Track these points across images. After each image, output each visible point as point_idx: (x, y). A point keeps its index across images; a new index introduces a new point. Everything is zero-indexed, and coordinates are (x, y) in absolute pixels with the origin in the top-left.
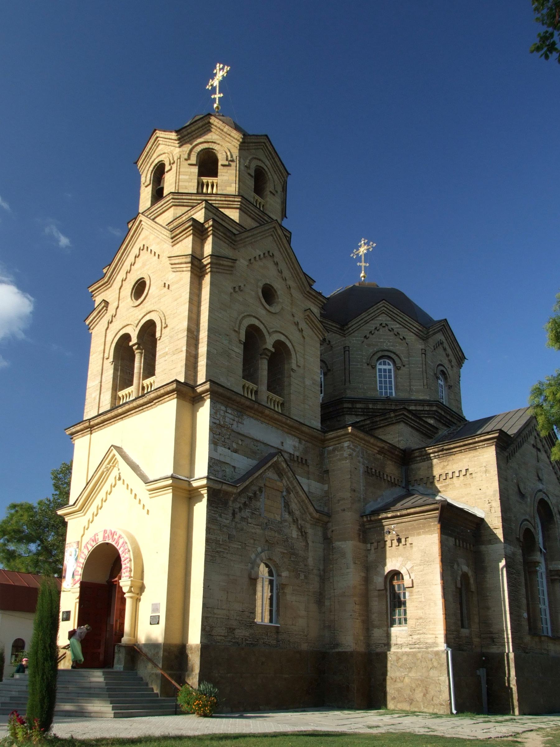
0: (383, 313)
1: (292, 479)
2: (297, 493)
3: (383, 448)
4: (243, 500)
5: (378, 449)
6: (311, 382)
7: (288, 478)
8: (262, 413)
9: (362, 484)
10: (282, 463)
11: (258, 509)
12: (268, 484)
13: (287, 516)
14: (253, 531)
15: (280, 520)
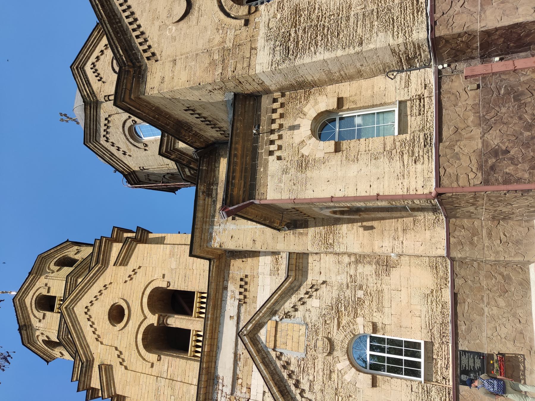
0: (96, 140)
1: (261, 315)
2: (274, 304)
3: (203, 192)
4: (293, 388)
5: (207, 199)
6: (173, 259)
7: (261, 318)
8: (208, 368)
9: (246, 227)
10: (248, 328)
11: (298, 361)
12: (272, 345)
13: (299, 314)
14: (321, 374)
15: (304, 327)
